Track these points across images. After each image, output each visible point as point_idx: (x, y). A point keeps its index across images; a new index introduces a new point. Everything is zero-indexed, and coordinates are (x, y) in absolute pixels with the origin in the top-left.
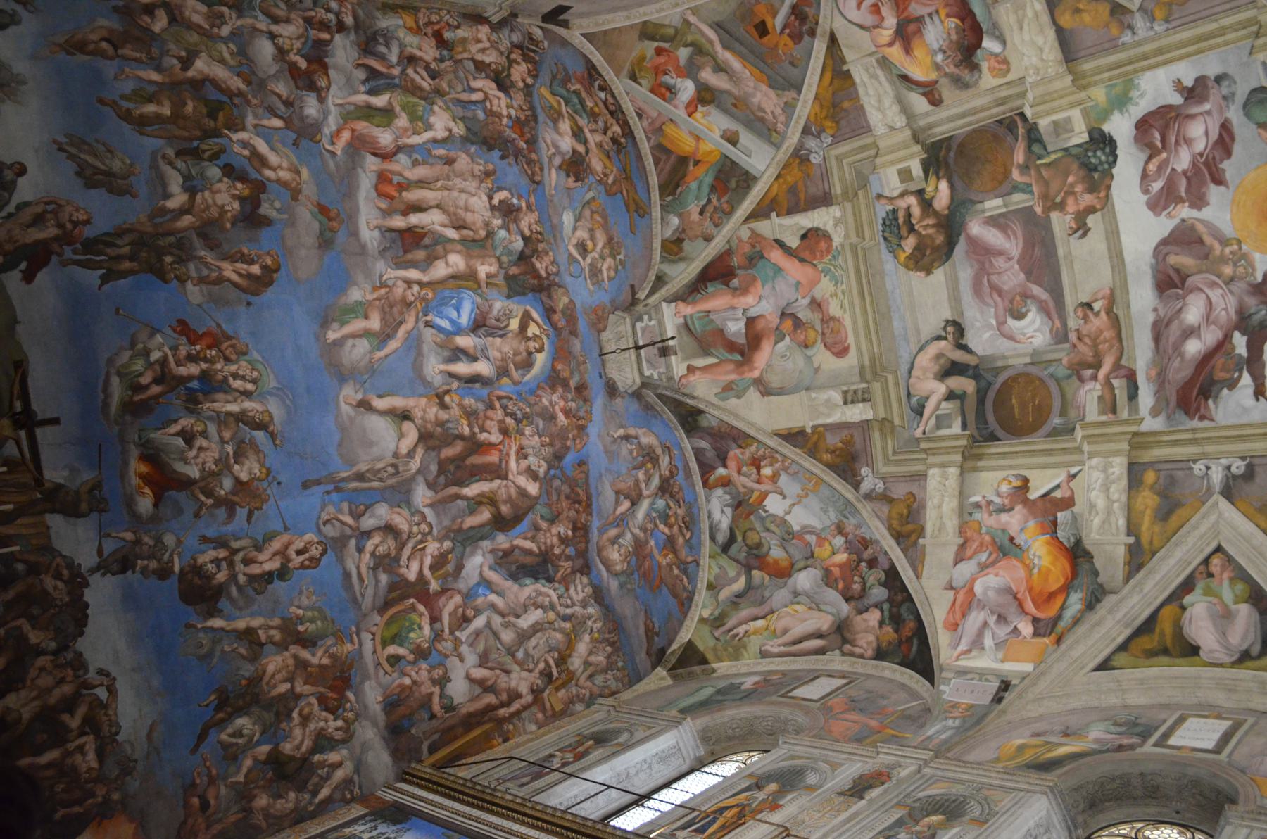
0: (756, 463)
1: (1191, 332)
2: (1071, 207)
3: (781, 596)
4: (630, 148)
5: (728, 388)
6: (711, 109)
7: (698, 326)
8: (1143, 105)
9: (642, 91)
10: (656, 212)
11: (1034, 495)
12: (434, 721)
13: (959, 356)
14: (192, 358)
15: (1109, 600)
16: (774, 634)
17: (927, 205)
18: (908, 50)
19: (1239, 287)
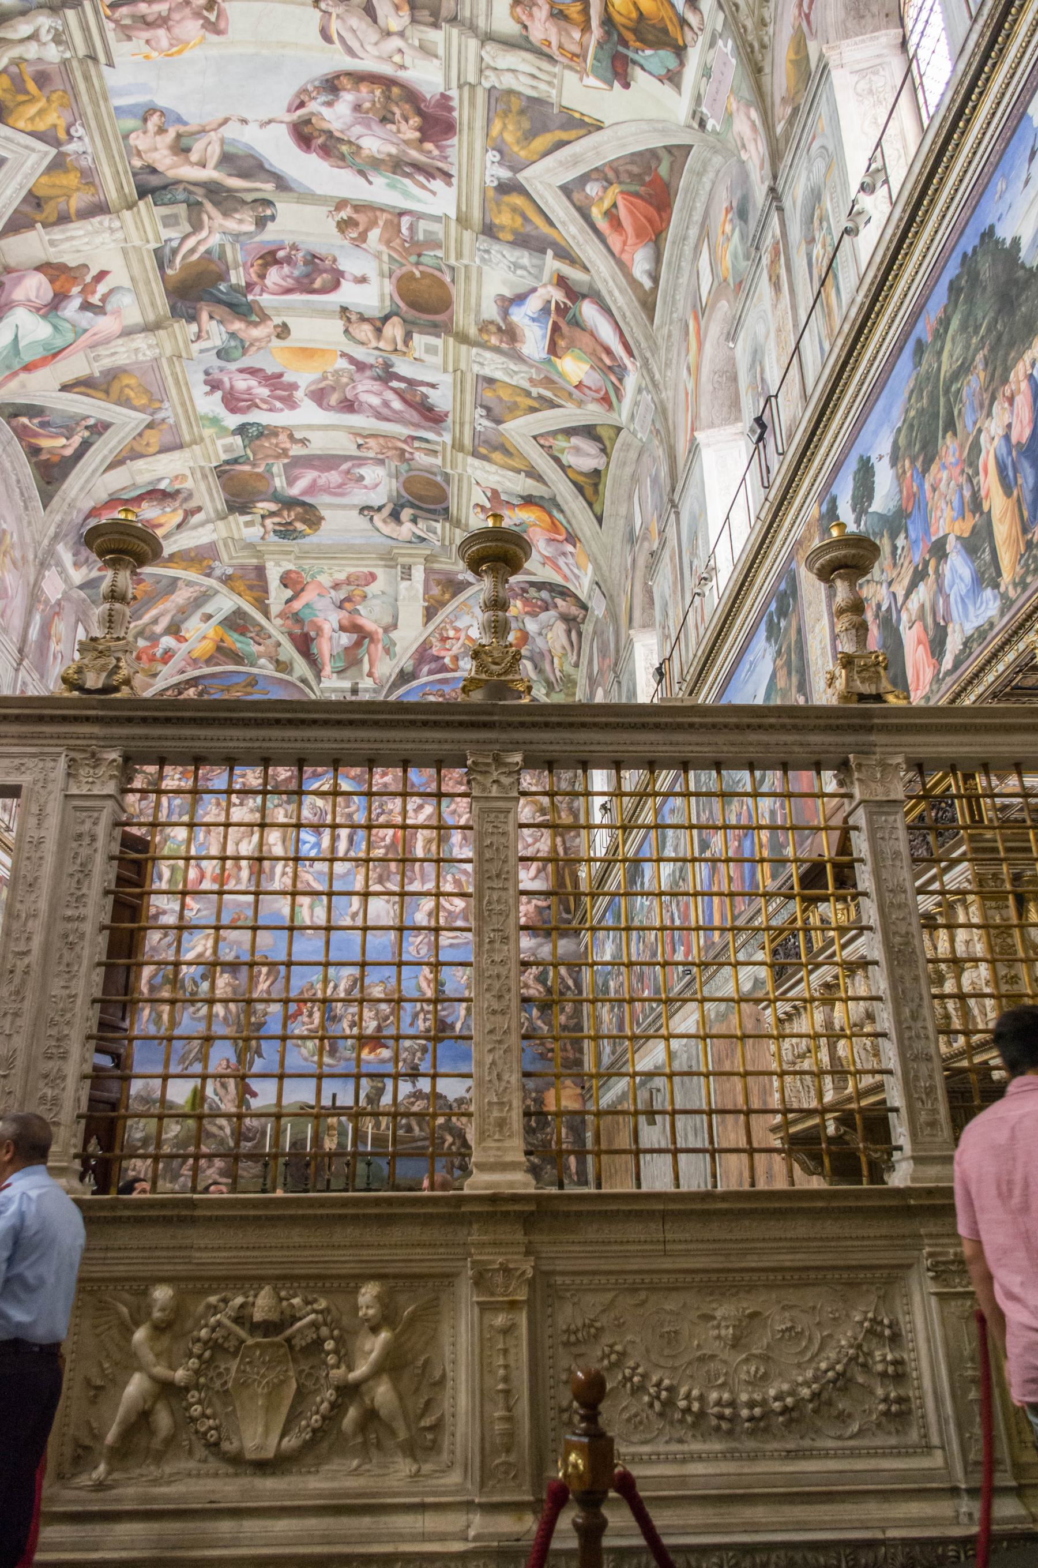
0: (444, 639)
1: (386, 404)
2: (288, 445)
3: (540, 642)
4: (206, 682)
5: (387, 651)
6: (184, 627)
7: (341, 664)
8: (221, 411)
9: (165, 670)
10: (255, 670)
11: (488, 505)
12: (554, 908)
13: (386, 512)
14: (310, 1015)
15: (559, 498)
16: (565, 655)
17: (272, 514)
18: (160, 525)
19: (357, 376)
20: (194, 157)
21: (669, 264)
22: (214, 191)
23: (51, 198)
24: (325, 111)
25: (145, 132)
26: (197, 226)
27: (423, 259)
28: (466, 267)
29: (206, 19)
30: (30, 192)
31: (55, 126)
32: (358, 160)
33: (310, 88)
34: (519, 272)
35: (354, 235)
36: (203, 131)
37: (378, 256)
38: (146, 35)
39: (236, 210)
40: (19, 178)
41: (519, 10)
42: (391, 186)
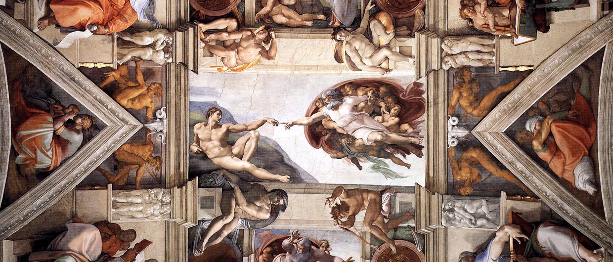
20: (236, 150)
21: (605, 169)
22: (245, 178)
23: (127, 164)
24: (333, 114)
25: (206, 125)
26: (226, 211)
27: (398, 234)
28: (434, 231)
29: (263, 48)
30: (114, 154)
31: (147, 108)
32: (353, 150)
33: (324, 97)
34: (479, 222)
35: (343, 220)
36: (246, 130)
37: (362, 238)
38: (222, 54)
39: (258, 199)
40: (110, 142)
41: (465, 11)
42: (376, 168)
